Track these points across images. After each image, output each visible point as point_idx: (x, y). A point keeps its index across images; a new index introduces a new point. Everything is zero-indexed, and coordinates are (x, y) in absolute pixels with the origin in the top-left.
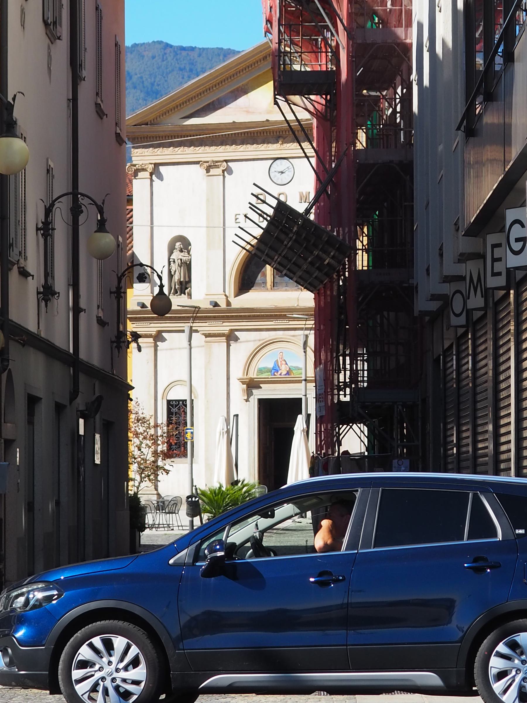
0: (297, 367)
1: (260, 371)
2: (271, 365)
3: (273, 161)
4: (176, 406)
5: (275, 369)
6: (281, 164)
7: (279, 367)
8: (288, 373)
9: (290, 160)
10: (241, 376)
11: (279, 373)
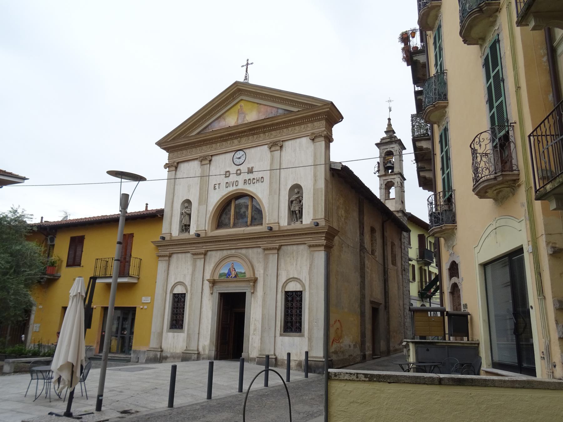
1: (221, 275)
2: (226, 272)
5: (229, 274)
8: (235, 277)
10: (209, 278)
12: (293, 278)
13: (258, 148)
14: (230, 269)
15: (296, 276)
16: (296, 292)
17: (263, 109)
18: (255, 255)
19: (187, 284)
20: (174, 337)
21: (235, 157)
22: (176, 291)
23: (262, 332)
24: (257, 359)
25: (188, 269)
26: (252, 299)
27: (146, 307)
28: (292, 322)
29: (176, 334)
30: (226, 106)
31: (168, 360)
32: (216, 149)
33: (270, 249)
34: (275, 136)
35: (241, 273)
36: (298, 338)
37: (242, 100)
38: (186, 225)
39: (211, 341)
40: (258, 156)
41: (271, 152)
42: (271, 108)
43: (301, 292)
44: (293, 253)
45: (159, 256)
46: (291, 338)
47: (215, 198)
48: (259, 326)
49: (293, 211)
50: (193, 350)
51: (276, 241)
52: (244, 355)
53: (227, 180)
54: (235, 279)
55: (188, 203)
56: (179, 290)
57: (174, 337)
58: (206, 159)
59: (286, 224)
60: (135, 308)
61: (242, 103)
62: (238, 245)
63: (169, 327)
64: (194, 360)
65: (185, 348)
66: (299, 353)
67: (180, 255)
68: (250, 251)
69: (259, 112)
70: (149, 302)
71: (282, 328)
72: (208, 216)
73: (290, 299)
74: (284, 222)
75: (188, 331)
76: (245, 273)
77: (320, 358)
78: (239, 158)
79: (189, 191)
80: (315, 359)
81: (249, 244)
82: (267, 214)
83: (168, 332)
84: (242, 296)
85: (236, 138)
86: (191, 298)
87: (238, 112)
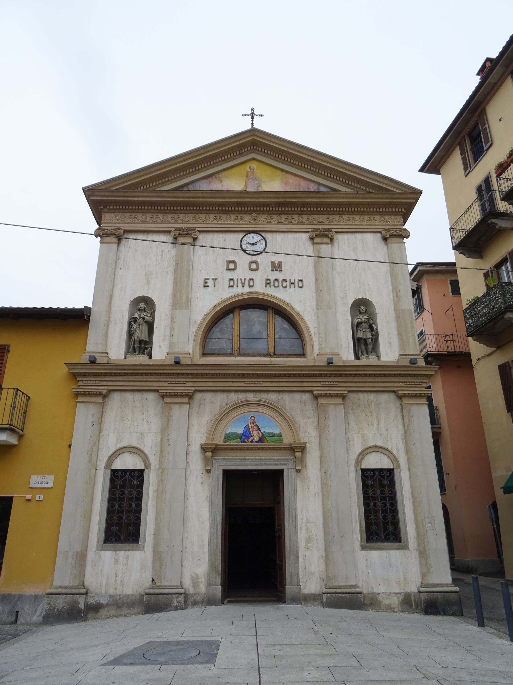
0: (271, 433)
1: (228, 437)
3: (245, 234)
4: (122, 477)
5: (246, 435)
6: (253, 238)
7: (250, 433)
8: (261, 440)
9: (263, 234)
11: (250, 439)
12: (376, 447)
13: (290, 235)
14: (247, 427)
15: (379, 444)
16: (381, 470)
17: (292, 180)
18: (297, 406)
19: (147, 451)
20: (116, 561)
21: (244, 242)
22: (119, 465)
23: (328, 543)
24: (325, 596)
25: (149, 423)
26: (298, 482)
27: (40, 497)
28: (381, 523)
29: (122, 553)
30: (225, 161)
31: (103, 612)
32: (207, 223)
33: (331, 396)
34: (322, 222)
35: (272, 435)
36: (398, 552)
37: (253, 159)
38: (141, 342)
39: (211, 565)
40: (290, 247)
41: (313, 244)
42: (306, 182)
43: (391, 472)
44: (369, 405)
45: (77, 395)
46: (384, 553)
47: (206, 302)
48: (318, 532)
49: (359, 339)
50: (171, 587)
51: (332, 383)
52: (290, 589)
53: (230, 275)
54: (261, 445)
55: (144, 305)
56: (127, 462)
57: (116, 561)
58: (189, 235)
59: (351, 357)
60: (11, 498)
61: (254, 165)
62: (264, 384)
63: (102, 538)
64: (177, 608)
65: (148, 583)
66: (402, 580)
67: (129, 396)
68: (286, 397)
69: (286, 184)
70: (50, 485)
71: (364, 535)
72: (194, 329)
73: (370, 482)
74: (347, 354)
75: (156, 545)
76: (280, 435)
77: (447, 585)
78: (253, 244)
79: (148, 283)
80: (435, 589)
81: (285, 385)
82: (315, 339)
83: (100, 549)
84: (275, 478)
85: (250, 212)
86: (161, 481)
87: (247, 176)
